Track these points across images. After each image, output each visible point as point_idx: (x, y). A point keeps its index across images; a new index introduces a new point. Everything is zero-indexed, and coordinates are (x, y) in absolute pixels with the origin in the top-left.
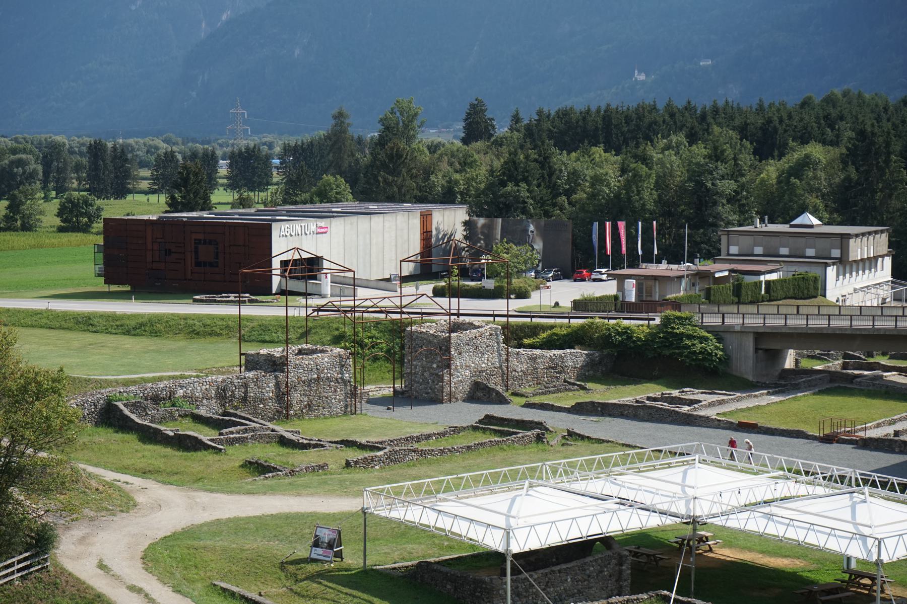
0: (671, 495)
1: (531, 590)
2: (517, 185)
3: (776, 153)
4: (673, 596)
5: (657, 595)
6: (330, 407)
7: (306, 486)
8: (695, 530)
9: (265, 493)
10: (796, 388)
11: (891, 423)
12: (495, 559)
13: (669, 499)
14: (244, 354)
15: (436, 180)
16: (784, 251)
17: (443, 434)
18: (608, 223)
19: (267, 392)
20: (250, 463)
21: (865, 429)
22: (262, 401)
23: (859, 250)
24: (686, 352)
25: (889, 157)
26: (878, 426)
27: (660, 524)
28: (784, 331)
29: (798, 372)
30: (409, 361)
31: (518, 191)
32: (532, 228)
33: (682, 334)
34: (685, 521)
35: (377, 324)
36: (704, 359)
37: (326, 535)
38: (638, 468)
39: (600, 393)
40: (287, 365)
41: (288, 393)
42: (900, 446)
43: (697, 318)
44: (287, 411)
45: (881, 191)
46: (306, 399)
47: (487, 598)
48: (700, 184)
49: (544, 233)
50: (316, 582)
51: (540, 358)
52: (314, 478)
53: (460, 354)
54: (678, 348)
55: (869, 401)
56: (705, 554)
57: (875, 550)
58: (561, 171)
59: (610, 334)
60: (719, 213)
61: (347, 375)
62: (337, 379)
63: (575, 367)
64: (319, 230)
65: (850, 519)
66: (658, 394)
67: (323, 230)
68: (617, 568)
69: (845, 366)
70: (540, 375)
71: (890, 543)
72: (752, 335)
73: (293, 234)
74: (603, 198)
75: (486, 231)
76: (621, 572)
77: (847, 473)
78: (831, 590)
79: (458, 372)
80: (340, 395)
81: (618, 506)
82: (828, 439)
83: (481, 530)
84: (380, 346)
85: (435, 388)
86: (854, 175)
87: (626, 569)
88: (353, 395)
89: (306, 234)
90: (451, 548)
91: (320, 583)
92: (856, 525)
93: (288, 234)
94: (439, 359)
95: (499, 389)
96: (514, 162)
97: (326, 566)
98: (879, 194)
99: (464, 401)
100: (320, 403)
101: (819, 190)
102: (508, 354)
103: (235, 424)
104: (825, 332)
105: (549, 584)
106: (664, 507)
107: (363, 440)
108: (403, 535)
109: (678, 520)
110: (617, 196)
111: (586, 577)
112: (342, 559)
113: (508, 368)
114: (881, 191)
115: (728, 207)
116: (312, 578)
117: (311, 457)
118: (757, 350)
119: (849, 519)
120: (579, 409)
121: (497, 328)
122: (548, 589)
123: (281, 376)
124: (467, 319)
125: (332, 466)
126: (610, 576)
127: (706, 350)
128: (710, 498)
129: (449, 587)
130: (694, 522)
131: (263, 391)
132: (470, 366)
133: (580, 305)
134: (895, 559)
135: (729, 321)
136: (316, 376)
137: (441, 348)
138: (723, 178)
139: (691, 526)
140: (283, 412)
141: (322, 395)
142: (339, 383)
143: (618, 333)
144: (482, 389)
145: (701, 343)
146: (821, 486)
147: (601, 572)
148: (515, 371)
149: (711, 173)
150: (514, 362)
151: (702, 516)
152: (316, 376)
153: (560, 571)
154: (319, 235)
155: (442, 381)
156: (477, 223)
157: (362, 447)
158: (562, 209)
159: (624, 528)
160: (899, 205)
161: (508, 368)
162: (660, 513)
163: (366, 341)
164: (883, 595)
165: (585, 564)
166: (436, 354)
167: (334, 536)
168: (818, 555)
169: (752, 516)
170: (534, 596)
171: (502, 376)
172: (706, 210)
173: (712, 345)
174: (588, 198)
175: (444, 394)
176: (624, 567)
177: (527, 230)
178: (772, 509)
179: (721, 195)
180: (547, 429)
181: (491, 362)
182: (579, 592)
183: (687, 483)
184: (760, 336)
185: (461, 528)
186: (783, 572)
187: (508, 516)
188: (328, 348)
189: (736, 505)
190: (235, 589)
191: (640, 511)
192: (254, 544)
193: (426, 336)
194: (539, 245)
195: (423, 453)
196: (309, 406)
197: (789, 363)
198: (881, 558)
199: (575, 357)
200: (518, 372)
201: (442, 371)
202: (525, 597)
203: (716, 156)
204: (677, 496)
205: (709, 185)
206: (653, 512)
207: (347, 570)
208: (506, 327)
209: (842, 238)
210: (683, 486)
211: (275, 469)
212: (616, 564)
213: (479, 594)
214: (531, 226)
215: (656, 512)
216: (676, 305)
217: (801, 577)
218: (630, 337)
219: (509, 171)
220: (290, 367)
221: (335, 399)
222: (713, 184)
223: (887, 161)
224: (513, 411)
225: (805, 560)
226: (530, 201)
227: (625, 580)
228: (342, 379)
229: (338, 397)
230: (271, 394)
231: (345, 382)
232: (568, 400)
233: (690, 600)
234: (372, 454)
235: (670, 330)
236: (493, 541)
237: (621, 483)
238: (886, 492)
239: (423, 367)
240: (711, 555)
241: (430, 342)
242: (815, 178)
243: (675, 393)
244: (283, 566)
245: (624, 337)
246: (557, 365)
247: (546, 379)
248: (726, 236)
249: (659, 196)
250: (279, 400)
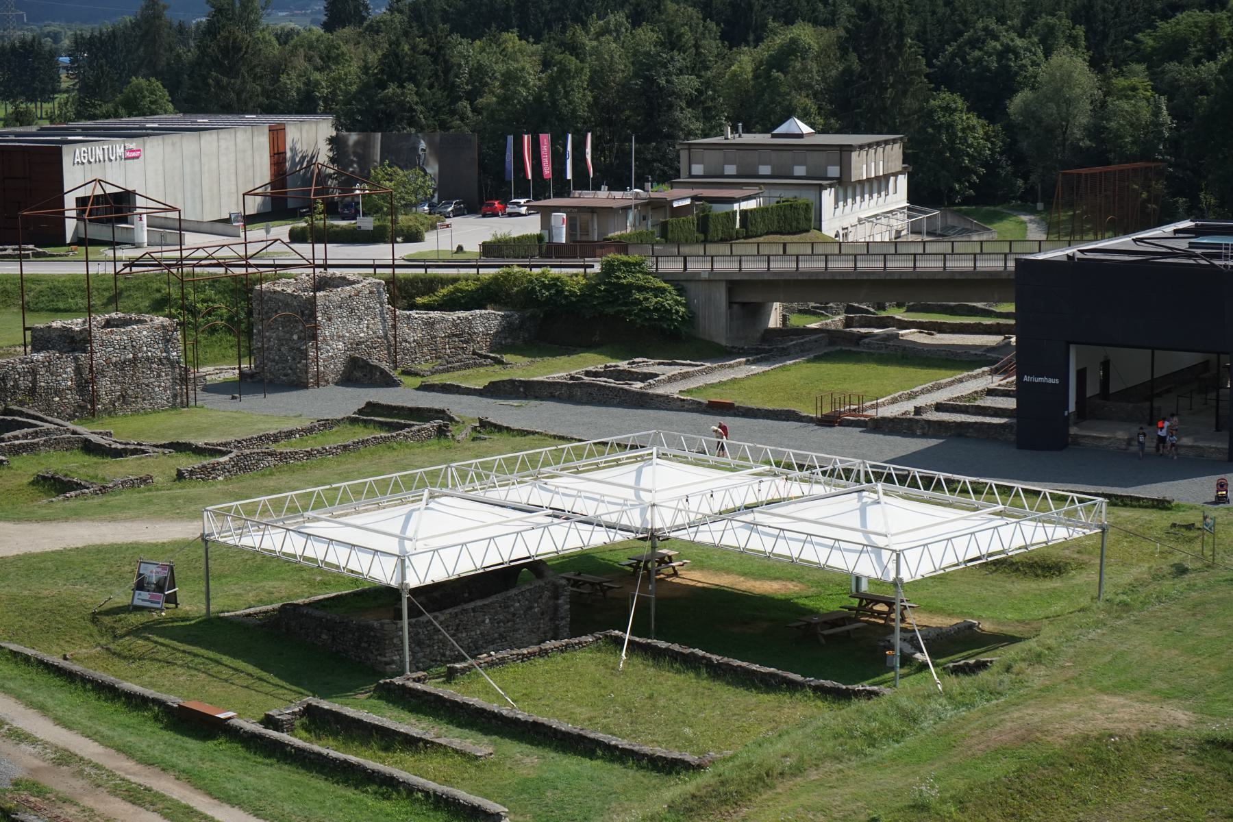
0: (622, 501)
1: (436, 637)
2: (401, 86)
3: (751, 37)
4: (627, 636)
5: (606, 636)
6: (153, 398)
7: (123, 508)
8: (654, 547)
9: (66, 520)
10: (784, 354)
11: (911, 397)
12: (385, 596)
13: (619, 508)
14: (29, 329)
15: (288, 82)
16: (765, 170)
17: (310, 430)
18: (526, 136)
19: (64, 380)
20: (44, 478)
21: (877, 406)
22: (58, 392)
23: (865, 166)
24: (636, 309)
25: (902, 40)
26: (894, 401)
27: (607, 541)
28: (766, 278)
29: (786, 332)
30: (259, 331)
31: (403, 94)
32: (423, 145)
33: (630, 285)
34: (641, 536)
35: (213, 282)
36: (660, 319)
37: (153, 573)
38: (576, 468)
39: (522, 368)
40: (90, 342)
41: (93, 381)
42: (923, 428)
43: (649, 263)
44: (93, 405)
45: (892, 86)
47: (377, 650)
48: (650, 80)
49: (440, 152)
50: (141, 638)
51: (439, 322)
52: (134, 496)
53: (330, 319)
54: (625, 304)
55: (881, 369)
56: (669, 580)
57: (892, 567)
58: (460, 66)
59: (534, 288)
60: (676, 121)
61: (175, 354)
62: (160, 360)
63: (488, 334)
64: (128, 154)
65: (858, 526)
66: (600, 368)
67: (134, 154)
68: (551, 603)
69: (848, 323)
70: (440, 346)
71: (911, 557)
72: (724, 284)
73: (92, 160)
74: (519, 102)
75: (360, 151)
76: (556, 608)
77: (854, 465)
78: (836, 620)
79: (327, 345)
80: (166, 381)
81: (550, 519)
82: (828, 421)
83: (366, 558)
84: (219, 312)
85: (297, 368)
86: (856, 65)
87: (564, 603)
88: (184, 380)
89: (110, 160)
90: (325, 584)
91: (148, 639)
92: (866, 533)
93: (85, 161)
94: (301, 328)
95: (385, 366)
96: (397, 56)
97: (155, 616)
98: (889, 90)
99: (337, 384)
100: (138, 393)
101: (809, 86)
102: (395, 318)
103: (21, 425)
104: (821, 278)
105: (461, 628)
106: (613, 519)
107: (200, 442)
108: (260, 568)
109: (631, 535)
110: (538, 99)
111: (509, 617)
112: (177, 604)
113: (395, 338)
114: (892, 86)
115: (689, 112)
116: (136, 632)
117: (129, 467)
118: (731, 304)
119: (858, 525)
120: (494, 390)
121: (379, 284)
122: (460, 635)
123: (83, 357)
124: (338, 272)
125: (158, 480)
126: (542, 614)
127: (664, 306)
128: (674, 504)
129: (324, 636)
130: (652, 537)
131: (59, 378)
132: (343, 337)
133: (492, 250)
134: (918, 577)
135: (693, 266)
137: (303, 313)
138: (681, 72)
139: (648, 543)
140: (88, 408)
141: (141, 381)
142: (163, 365)
143: (544, 286)
144: (362, 367)
145: (656, 297)
146: (820, 483)
147: (531, 608)
148: (406, 341)
149: (665, 66)
150: (403, 328)
151: (663, 529)
152: (131, 356)
153: (474, 610)
154: (128, 161)
155: (306, 357)
156: (348, 139)
157: (198, 451)
158: (463, 118)
159: (560, 549)
160: (916, 106)
161: (395, 338)
162: (607, 527)
163: (199, 305)
164: (904, 625)
165: (509, 598)
166: (297, 322)
167: (165, 573)
168: (818, 576)
169: (729, 526)
170: (441, 645)
171: (388, 349)
172: (659, 116)
173: (671, 299)
174: (498, 103)
175: (310, 375)
176: (560, 602)
177: (416, 149)
178: (757, 516)
179: (679, 97)
180: (451, 419)
181: (372, 329)
182: (502, 637)
183: (642, 485)
184: (735, 285)
185: (338, 556)
186: (772, 599)
187: (402, 539)
188: (147, 317)
189: (708, 512)
190: (29, 652)
191: (580, 526)
192: (52, 589)
193: (281, 297)
194: (433, 169)
195: (283, 457)
197: (774, 321)
198: (901, 576)
199: (486, 320)
200: (409, 343)
201: (306, 344)
202: (429, 646)
203: (670, 43)
204: (629, 503)
205: (663, 82)
206: (598, 525)
207: (183, 620)
208: (391, 282)
209: (841, 151)
210: (637, 489)
211: (79, 486)
212: (549, 598)
213: (366, 645)
214: (422, 142)
215: (601, 526)
216: (621, 246)
217: (796, 605)
218: (560, 292)
219: (389, 67)
220: (95, 345)
222: (668, 81)
223: (900, 46)
224: (405, 395)
225: (800, 582)
226: (419, 108)
227: (562, 619)
228: (167, 358)
229: (163, 384)
230: (70, 383)
231: (172, 364)
232: (479, 378)
233: (649, 641)
234: (213, 460)
235: (614, 280)
236: (383, 573)
237: (553, 488)
238: (905, 489)
239: (279, 340)
240: (676, 580)
241: (287, 305)
242: (804, 70)
243: (623, 365)
244: (95, 617)
245: (553, 291)
246: (463, 331)
247: (448, 351)
248: (687, 152)
249: (596, 98)
250: (81, 390)
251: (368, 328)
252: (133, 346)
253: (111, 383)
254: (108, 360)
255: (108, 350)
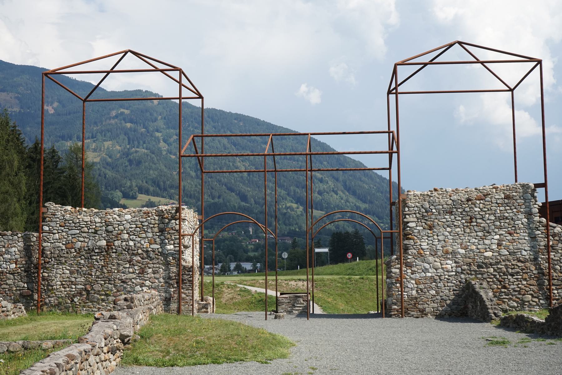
46: (82, 280)
99: (440, 317)
132: (454, 253)
136: (104, 243)
142: (152, 259)
152: (104, 243)
171: (538, 279)
196: (88, 292)
221: (142, 285)
230: (13, 266)
251: (499, 245)
252: (107, 231)
253: (72, 273)
254: (69, 245)
255: (70, 232)
